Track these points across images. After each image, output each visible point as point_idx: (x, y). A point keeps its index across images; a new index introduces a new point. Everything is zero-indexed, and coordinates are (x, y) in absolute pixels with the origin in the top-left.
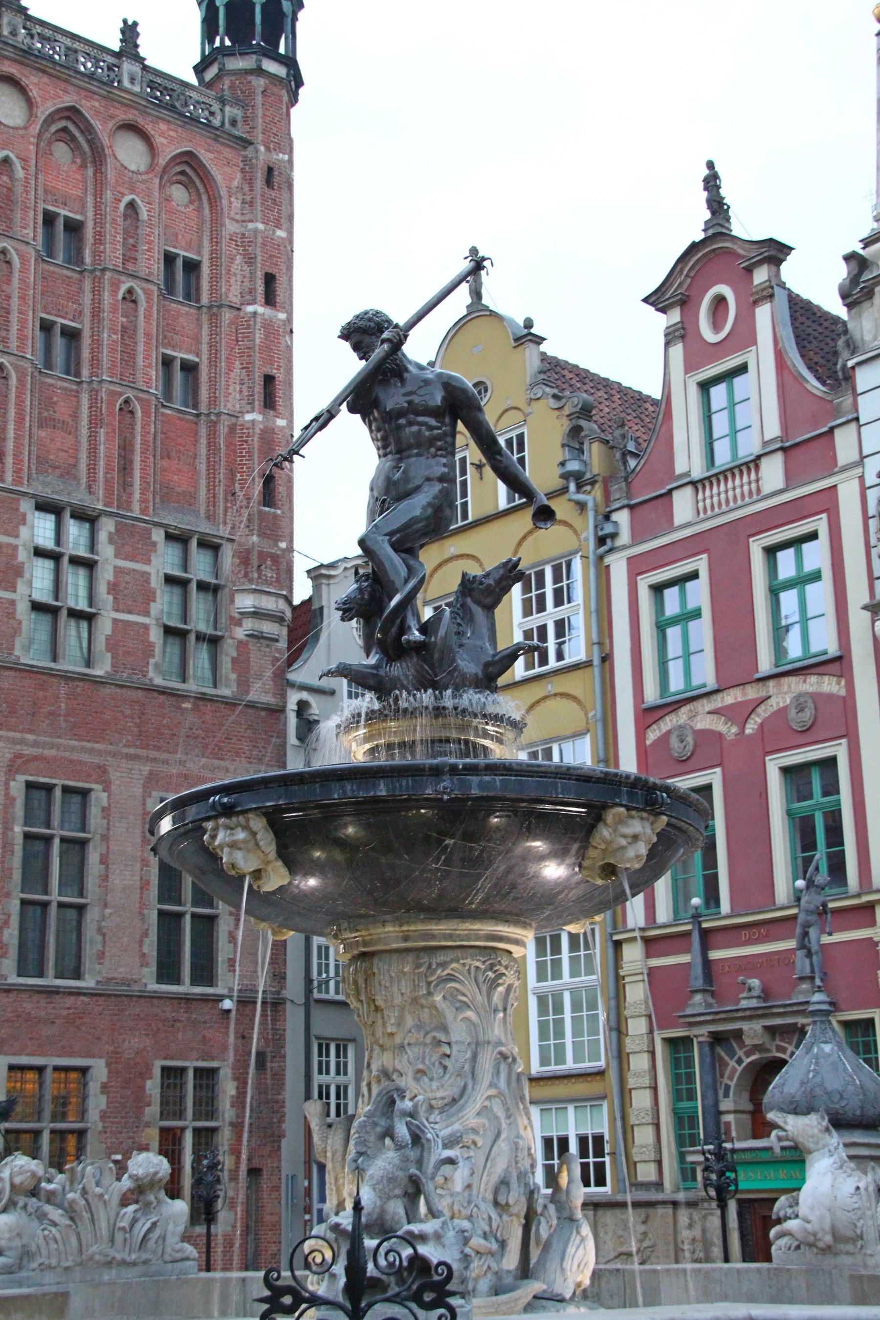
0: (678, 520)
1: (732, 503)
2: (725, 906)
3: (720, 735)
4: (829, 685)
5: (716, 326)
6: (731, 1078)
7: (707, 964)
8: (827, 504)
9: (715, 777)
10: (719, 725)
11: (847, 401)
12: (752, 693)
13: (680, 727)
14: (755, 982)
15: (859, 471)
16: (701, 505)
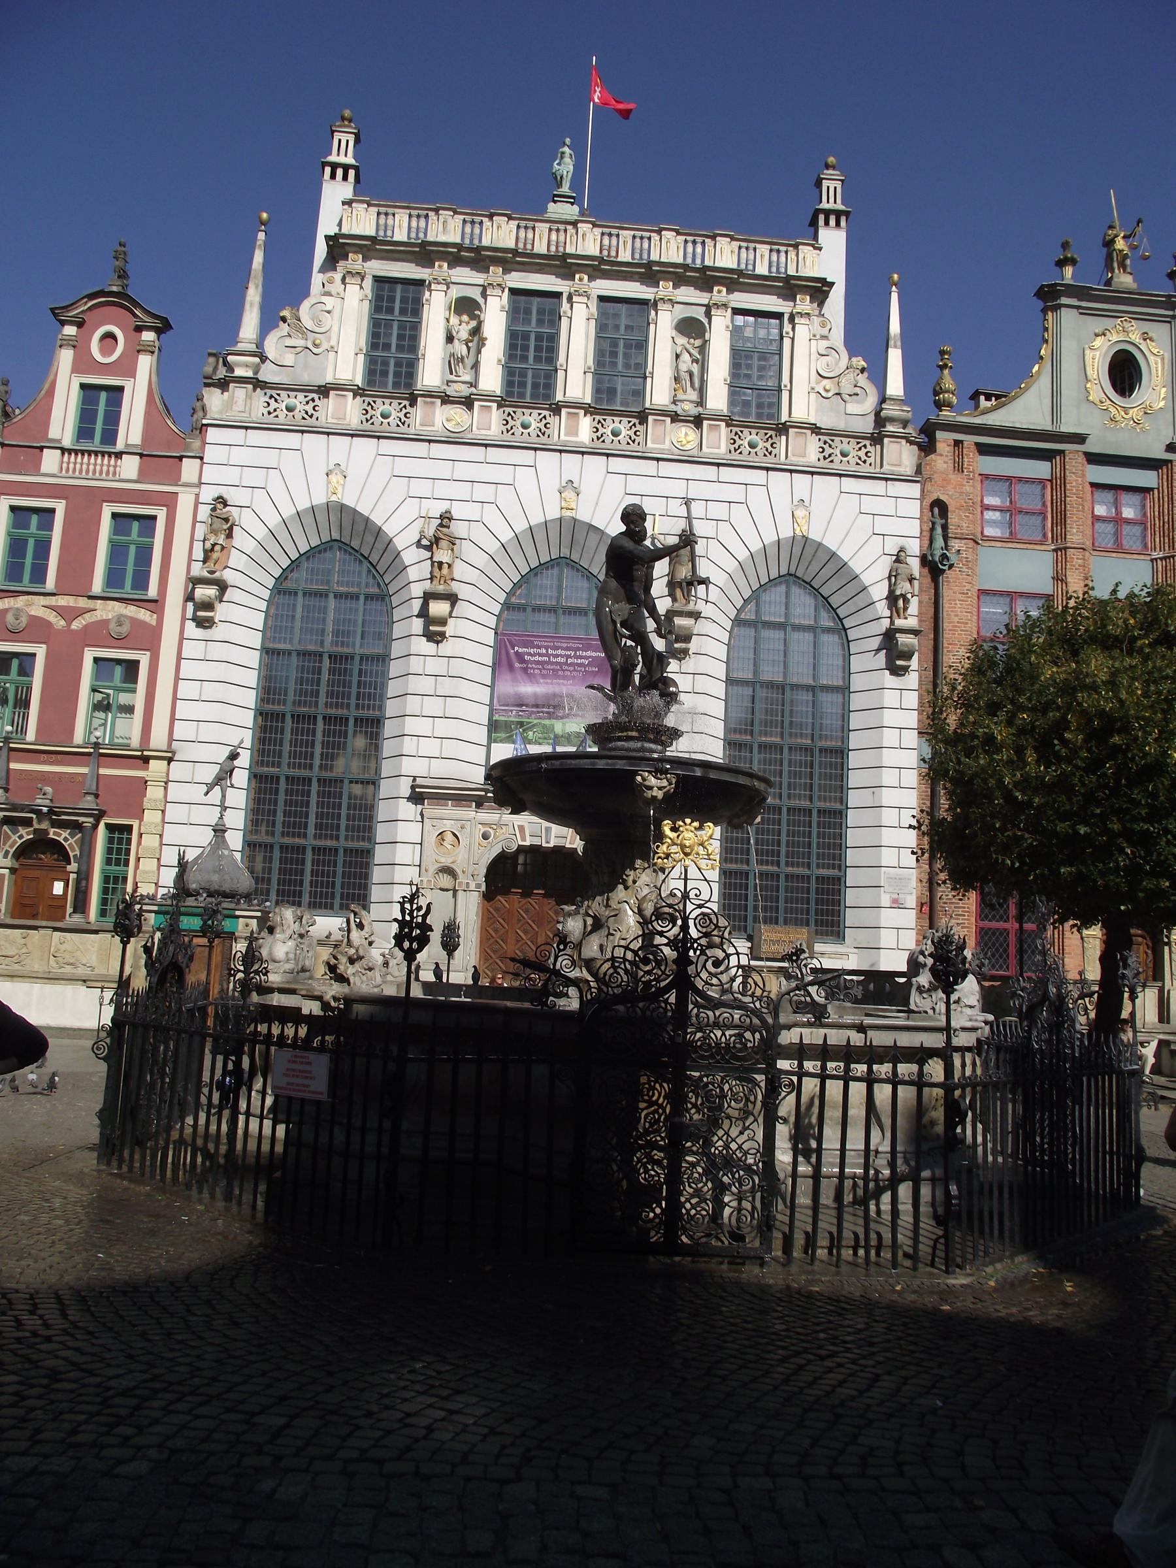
0: (44, 469)
1: (91, 472)
2: (31, 736)
3: (49, 624)
4: (144, 615)
5: (105, 352)
6: (11, 847)
7: (8, 770)
8: (170, 501)
9: (41, 651)
10: (51, 617)
11: (196, 444)
12: (83, 603)
13: (18, 609)
14: (49, 789)
15: (196, 490)
16: (65, 465)
